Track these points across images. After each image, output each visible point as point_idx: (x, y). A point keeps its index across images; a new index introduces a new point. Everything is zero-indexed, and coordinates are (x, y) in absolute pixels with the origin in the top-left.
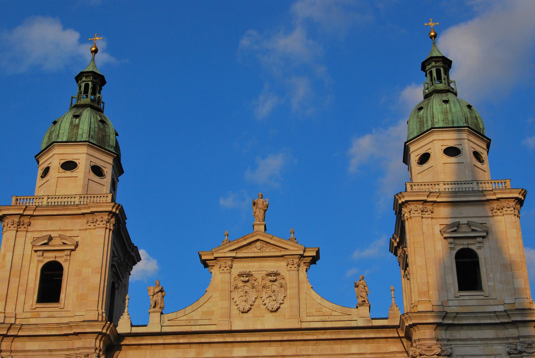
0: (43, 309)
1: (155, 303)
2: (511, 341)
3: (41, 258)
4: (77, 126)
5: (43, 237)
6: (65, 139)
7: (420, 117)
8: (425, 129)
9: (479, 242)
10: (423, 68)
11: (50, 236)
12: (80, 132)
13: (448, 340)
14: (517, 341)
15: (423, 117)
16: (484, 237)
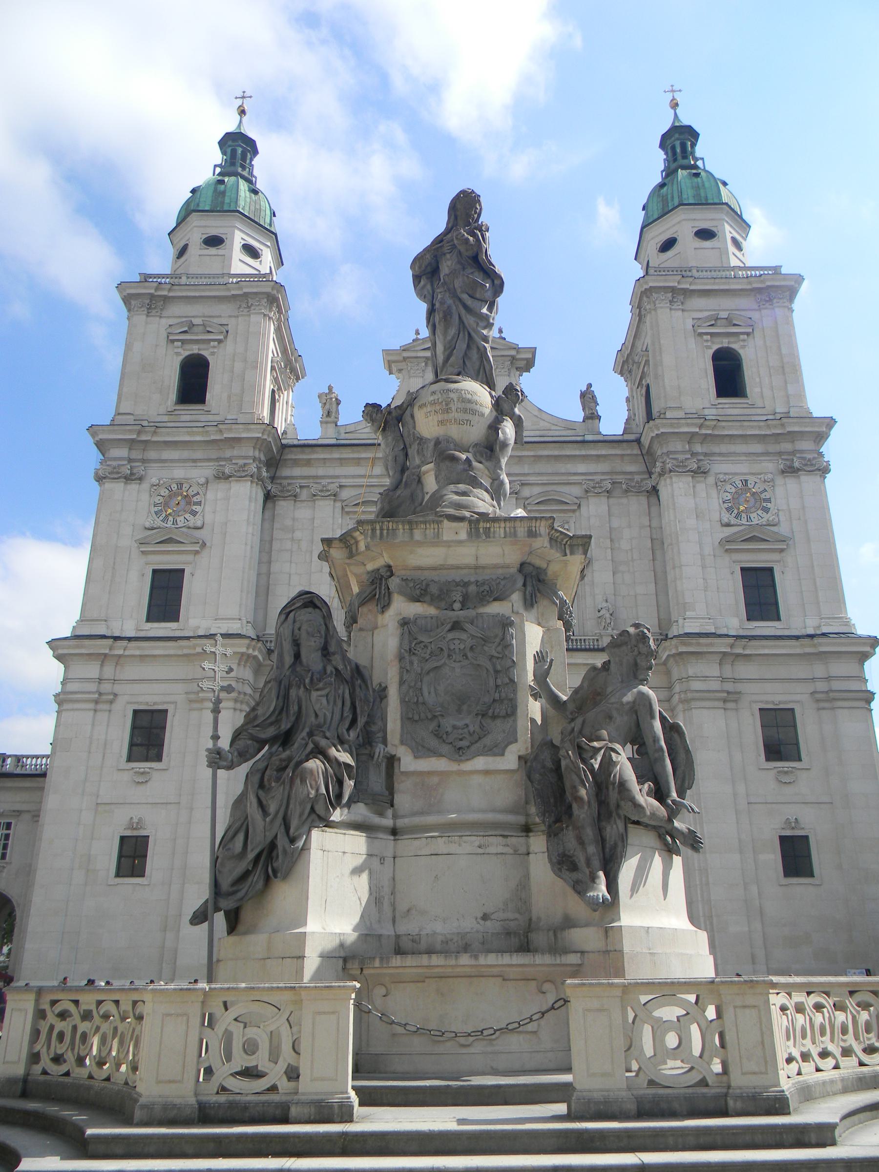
0: (183, 412)
1: (329, 412)
2: (783, 457)
3: (180, 350)
4: (223, 193)
5: (182, 322)
6: (207, 208)
7: (663, 197)
8: (670, 208)
9: (744, 340)
10: (662, 146)
11: (191, 321)
12: (227, 200)
13: (706, 455)
14: (791, 457)
15: (667, 195)
16: (748, 334)
